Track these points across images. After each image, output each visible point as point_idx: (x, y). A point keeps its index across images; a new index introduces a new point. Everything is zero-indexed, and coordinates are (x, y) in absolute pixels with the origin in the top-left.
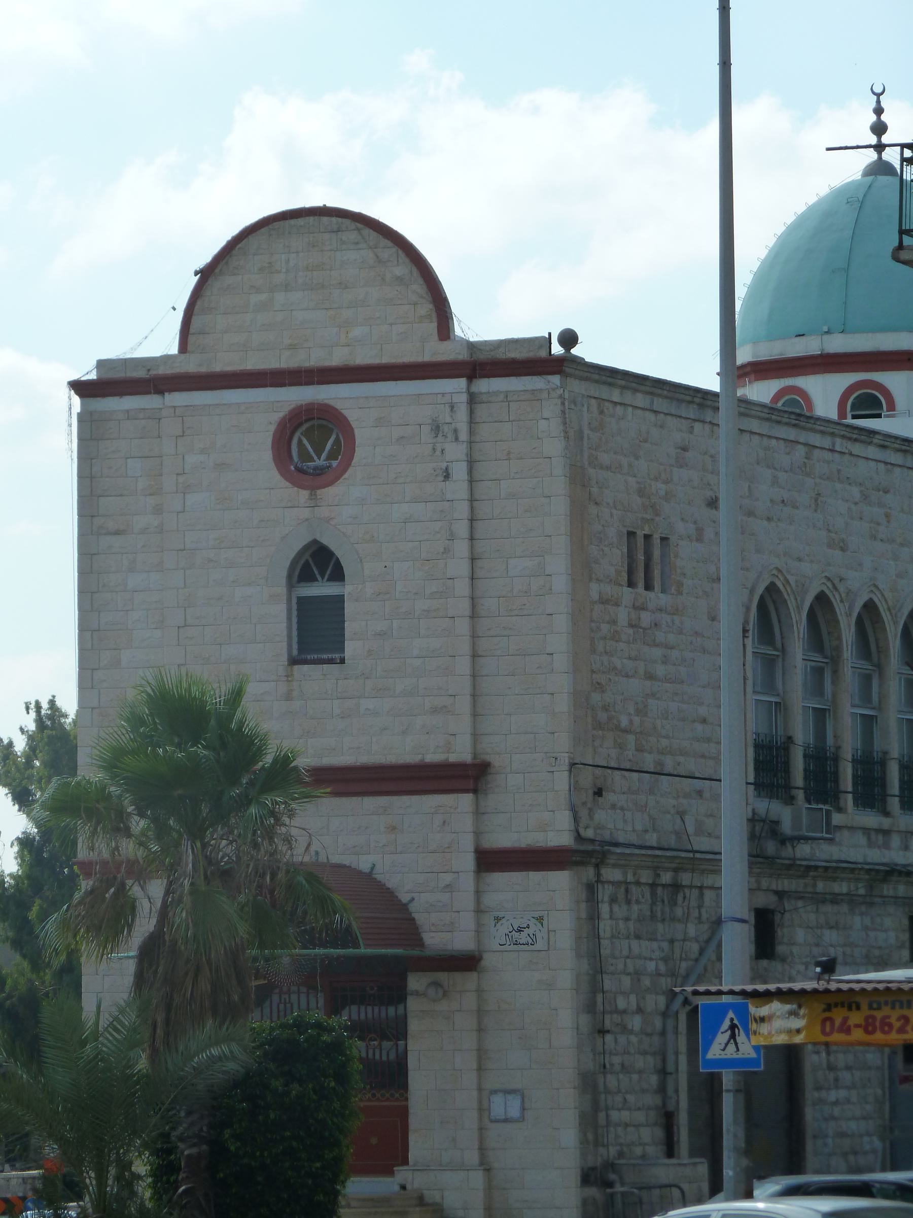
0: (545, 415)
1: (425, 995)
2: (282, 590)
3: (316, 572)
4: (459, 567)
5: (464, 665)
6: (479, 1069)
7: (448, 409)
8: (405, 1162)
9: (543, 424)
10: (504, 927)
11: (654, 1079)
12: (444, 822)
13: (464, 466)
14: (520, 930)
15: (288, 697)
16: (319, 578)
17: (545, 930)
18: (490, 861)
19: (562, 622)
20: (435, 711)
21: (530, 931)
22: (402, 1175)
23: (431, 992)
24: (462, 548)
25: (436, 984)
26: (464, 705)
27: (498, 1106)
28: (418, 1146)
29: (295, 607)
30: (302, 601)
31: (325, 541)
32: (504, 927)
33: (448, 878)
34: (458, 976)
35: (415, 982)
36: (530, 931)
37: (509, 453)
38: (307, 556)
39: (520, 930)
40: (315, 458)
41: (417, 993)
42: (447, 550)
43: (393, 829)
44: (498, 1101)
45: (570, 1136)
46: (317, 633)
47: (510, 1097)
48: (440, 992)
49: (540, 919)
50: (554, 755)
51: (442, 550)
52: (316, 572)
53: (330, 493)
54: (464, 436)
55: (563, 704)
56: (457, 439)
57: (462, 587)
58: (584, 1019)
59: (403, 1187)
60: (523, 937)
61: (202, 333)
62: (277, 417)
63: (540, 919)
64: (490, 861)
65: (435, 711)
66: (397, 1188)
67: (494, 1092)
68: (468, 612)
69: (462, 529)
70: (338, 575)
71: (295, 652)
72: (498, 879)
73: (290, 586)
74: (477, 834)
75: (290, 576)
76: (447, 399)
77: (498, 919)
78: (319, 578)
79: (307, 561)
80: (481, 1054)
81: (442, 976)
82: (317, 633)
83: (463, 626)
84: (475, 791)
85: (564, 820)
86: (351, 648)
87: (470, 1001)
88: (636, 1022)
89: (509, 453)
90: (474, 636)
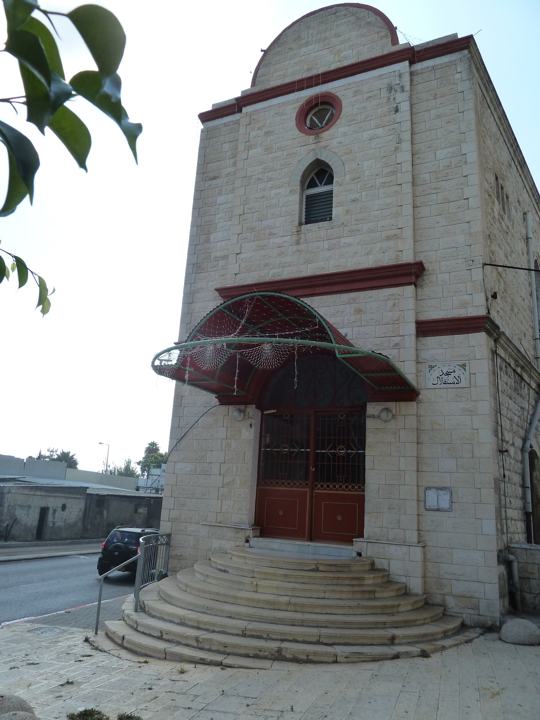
0: (459, 71)
1: (379, 417)
2: (298, 188)
3: (318, 182)
4: (405, 156)
5: (408, 210)
6: (418, 471)
7: (397, 77)
8: (362, 536)
9: (458, 76)
10: (437, 372)
11: (520, 490)
12: (394, 304)
13: (408, 104)
14: (448, 374)
15: (298, 243)
16: (319, 185)
17: (467, 374)
18: (426, 329)
19: (474, 179)
20: (388, 238)
21: (456, 374)
22: (358, 544)
23: (384, 415)
24: (406, 146)
25: (387, 410)
26: (408, 232)
27: (432, 498)
28: (370, 525)
29: (305, 200)
30: (308, 197)
31: (322, 158)
32: (437, 372)
33: (397, 340)
34: (403, 404)
35: (372, 409)
36: (456, 374)
37: (436, 95)
38: (312, 175)
39: (448, 374)
40: (319, 125)
41: (373, 416)
42: (396, 149)
43: (359, 311)
44: (432, 495)
45: (490, 526)
46: (317, 209)
47: (441, 493)
48: (390, 415)
49: (464, 366)
50: (472, 259)
51: (394, 149)
52: (318, 182)
53: (325, 135)
54: (407, 88)
55: (478, 227)
56: (403, 91)
57: (407, 167)
58: (494, 439)
59: (359, 554)
60: (451, 379)
61: (263, 75)
62: (299, 104)
63: (464, 366)
64: (426, 329)
65: (388, 238)
66: (354, 554)
67: (430, 488)
68: (410, 180)
69: (407, 136)
70: (330, 181)
71: (304, 220)
72: (431, 341)
73: (302, 190)
74: (417, 313)
75: (302, 182)
76: (397, 74)
77: (431, 367)
78: (319, 185)
79: (313, 177)
80: (419, 460)
81: (392, 405)
82: (317, 209)
83: (408, 188)
84: (416, 286)
85: (480, 299)
86: (335, 211)
87: (412, 422)
88: (512, 450)
89: (436, 95)
90: (414, 196)
